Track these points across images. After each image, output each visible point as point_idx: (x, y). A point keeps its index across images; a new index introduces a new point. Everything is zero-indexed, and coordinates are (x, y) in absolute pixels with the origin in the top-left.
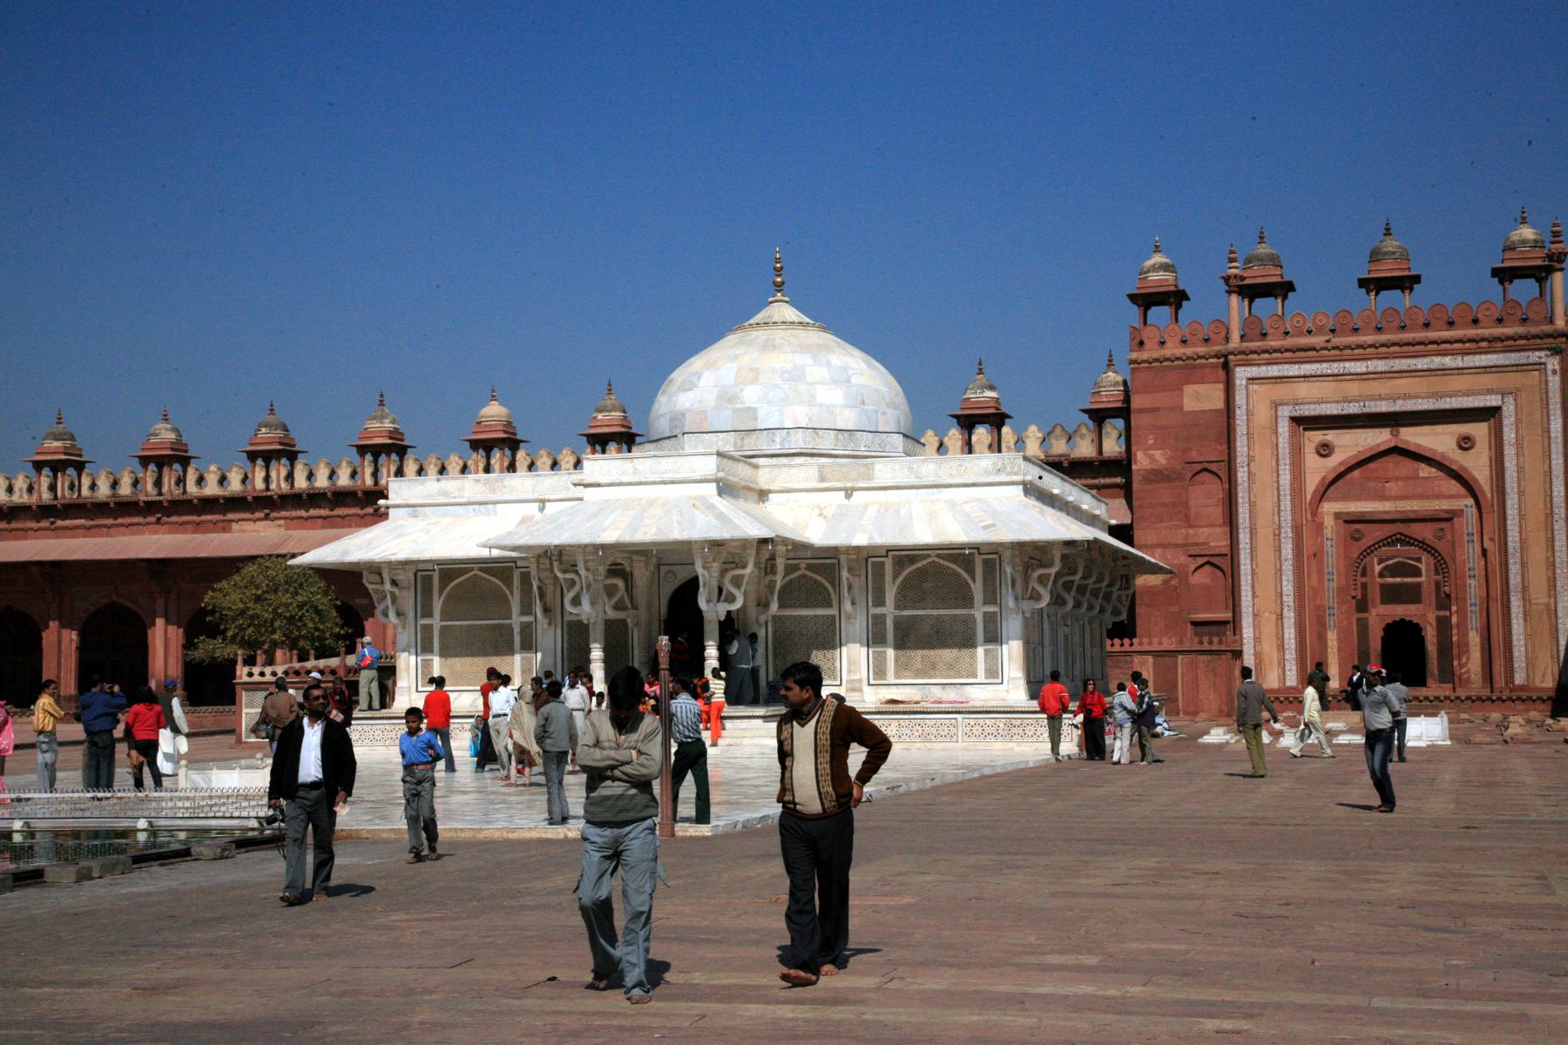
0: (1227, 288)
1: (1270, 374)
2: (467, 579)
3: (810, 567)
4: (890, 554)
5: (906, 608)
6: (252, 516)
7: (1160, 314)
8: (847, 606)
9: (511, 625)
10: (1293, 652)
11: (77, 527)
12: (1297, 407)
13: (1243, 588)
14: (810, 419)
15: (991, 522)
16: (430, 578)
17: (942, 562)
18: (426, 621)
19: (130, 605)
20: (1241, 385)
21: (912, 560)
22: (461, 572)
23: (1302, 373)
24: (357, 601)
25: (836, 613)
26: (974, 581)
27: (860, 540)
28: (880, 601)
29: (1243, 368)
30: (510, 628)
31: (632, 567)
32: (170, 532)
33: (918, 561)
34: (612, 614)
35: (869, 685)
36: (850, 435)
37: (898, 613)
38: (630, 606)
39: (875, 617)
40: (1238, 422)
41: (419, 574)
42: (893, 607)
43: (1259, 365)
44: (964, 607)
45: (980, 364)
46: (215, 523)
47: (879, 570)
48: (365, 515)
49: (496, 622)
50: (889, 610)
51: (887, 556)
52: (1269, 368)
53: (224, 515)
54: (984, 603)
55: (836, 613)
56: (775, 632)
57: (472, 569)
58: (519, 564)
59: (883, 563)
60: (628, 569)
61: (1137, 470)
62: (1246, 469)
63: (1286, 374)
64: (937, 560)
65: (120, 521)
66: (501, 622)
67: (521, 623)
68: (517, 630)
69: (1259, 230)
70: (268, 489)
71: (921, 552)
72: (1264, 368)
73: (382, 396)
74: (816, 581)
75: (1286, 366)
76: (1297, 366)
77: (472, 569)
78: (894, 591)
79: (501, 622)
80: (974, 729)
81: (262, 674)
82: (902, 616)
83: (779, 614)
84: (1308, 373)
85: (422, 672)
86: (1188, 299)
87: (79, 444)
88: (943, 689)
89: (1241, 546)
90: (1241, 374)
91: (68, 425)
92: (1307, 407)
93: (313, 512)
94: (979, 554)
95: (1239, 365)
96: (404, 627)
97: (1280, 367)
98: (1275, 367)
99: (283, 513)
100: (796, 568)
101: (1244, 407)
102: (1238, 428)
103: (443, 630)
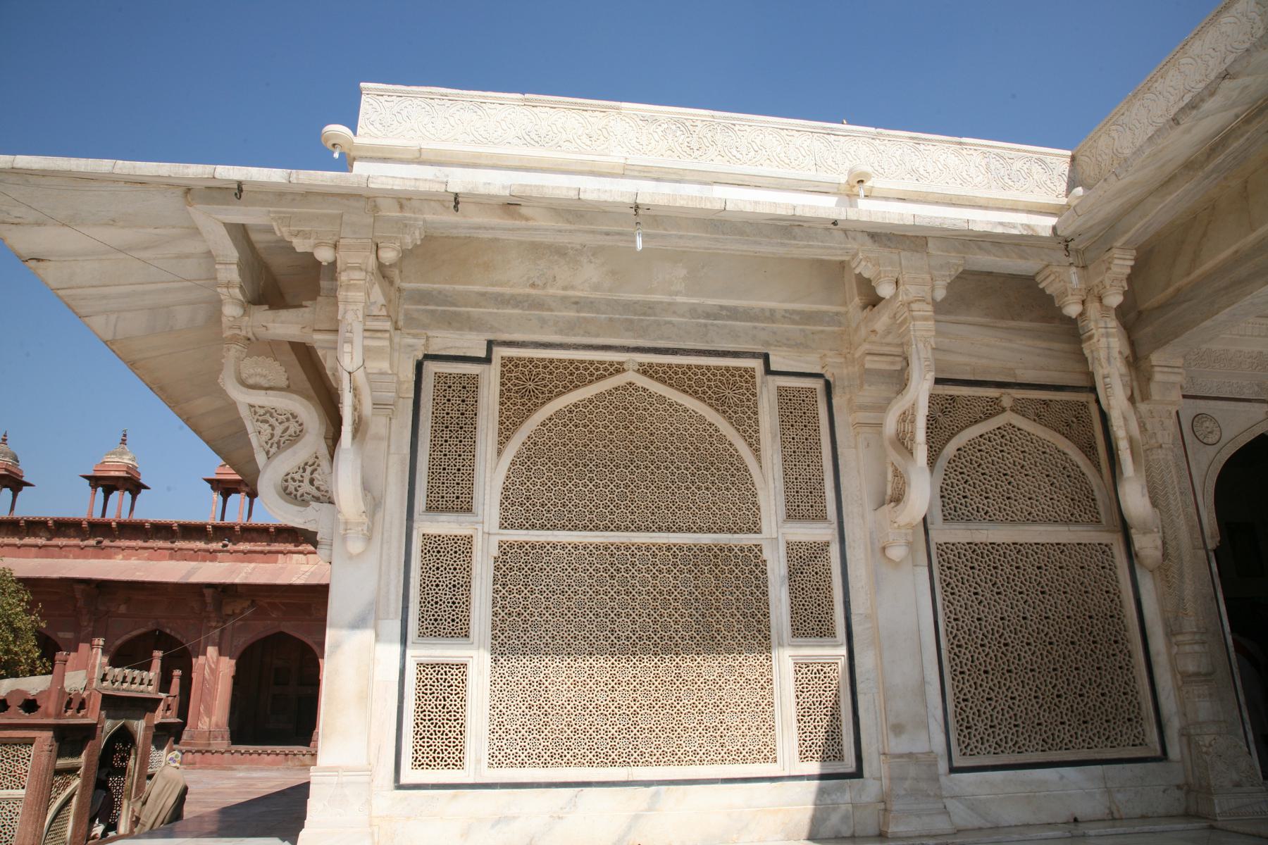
2: (600, 396)
16: (470, 386)
18: (446, 526)
22: (579, 375)
24: (61, 635)
30: (753, 562)
41: (431, 368)
48: (86, 546)
49: (706, 539)
57: (619, 369)
68: (777, 569)
73: (125, 435)
77: (619, 369)
85: (420, 710)
93: (27, 540)
96: (369, 539)
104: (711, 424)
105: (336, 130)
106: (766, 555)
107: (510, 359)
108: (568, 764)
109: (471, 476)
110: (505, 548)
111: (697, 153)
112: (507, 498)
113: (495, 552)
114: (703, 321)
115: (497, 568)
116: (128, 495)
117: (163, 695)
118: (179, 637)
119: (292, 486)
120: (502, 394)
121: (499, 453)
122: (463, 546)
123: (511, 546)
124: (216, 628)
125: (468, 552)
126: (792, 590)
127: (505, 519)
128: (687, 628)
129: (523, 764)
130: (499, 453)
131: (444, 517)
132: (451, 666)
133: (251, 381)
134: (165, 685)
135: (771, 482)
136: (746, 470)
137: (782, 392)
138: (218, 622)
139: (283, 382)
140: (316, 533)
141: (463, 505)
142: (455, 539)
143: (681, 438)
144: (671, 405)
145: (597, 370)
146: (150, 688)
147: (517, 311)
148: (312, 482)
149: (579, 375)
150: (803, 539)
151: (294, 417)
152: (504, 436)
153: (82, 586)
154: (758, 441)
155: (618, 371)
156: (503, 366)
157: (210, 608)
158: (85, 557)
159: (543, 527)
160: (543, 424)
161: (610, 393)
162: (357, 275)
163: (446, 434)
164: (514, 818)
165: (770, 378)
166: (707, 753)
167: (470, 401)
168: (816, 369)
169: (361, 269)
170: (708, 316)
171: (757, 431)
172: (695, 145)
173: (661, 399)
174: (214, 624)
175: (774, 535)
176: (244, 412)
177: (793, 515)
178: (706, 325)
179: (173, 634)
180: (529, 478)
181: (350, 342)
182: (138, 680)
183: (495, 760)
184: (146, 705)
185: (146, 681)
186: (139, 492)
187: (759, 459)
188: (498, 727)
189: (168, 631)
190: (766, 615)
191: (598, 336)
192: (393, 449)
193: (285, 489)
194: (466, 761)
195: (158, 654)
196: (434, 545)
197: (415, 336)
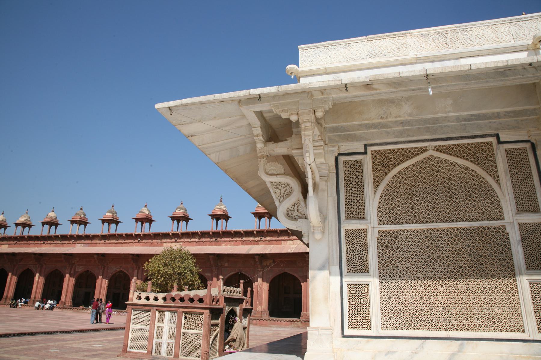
2: (417, 163)
6: (171, 241)
11: (112, 243)
16: (359, 165)
18: (355, 225)
19: (126, 272)
24: (206, 274)
32: (142, 246)
41: (342, 159)
46: (158, 243)
48: (212, 241)
49: (476, 224)
53: (161, 240)
57: (425, 150)
65: (126, 241)
66: (485, 223)
68: (515, 237)
73: (221, 198)
77: (425, 150)
79: (485, 223)
81: (148, 298)
85: (350, 304)
87: (118, 215)
91: (115, 209)
93: (193, 240)
96: (323, 232)
99: (182, 240)
103: (383, 237)
104: (472, 171)
105: (291, 67)
106: (508, 230)
107: (375, 151)
108: (418, 329)
109: (363, 203)
110: (382, 234)
111: (450, 46)
112: (380, 212)
113: (377, 235)
114: (463, 123)
115: (379, 242)
116: (224, 221)
117: (245, 297)
118: (247, 275)
119: (290, 213)
120: (373, 167)
121: (375, 192)
122: (363, 234)
123: (384, 232)
124: (260, 271)
125: (365, 236)
126: (524, 247)
127: (380, 221)
128: (470, 266)
129: (397, 328)
130: (375, 192)
131: (354, 222)
132: (362, 285)
133: (270, 172)
134: (245, 294)
135: (507, 195)
136: (493, 190)
137: (507, 151)
138: (261, 269)
139: (283, 172)
140: (301, 232)
141: (361, 216)
142: (359, 231)
143: (458, 178)
144: (452, 163)
145: (415, 151)
146: (240, 295)
147: (375, 130)
148: (298, 211)
150: (528, 221)
151: (288, 185)
152: (376, 184)
153: (212, 256)
154: (498, 176)
155: (424, 151)
156: (372, 154)
157: (258, 263)
158: (212, 245)
159: (397, 223)
160: (393, 178)
161: (422, 161)
162: (308, 124)
163: (351, 186)
164: (395, 352)
165: (501, 145)
166: (486, 326)
167: (360, 171)
168: (526, 138)
169: (309, 122)
170: (465, 120)
171: (497, 172)
172: (449, 42)
173: (447, 161)
174: (260, 270)
175: (512, 221)
176: (269, 185)
177: (520, 210)
178: (465, 125)
179: (245, 274)
180: (389, 202)
181: (308, 152)
182: (236, 292)
183: (384, 326)
184: (239, 301)
185: (238, 292)
186: (228, 220)
187: (499, 184)
188: (384, 311)
189: (243, 273)
190: (511, 259)
191: (413, 136)
192: (329, 195)
193: (288, 214)
194: (372, 326)
195: (242, 282)
196: (350, 234)
197: (334, 146)
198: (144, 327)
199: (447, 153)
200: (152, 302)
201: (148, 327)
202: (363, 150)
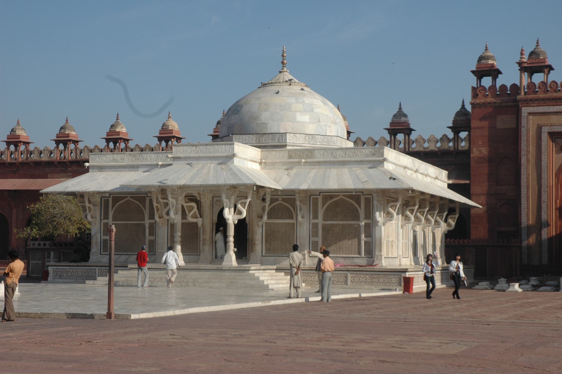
0: (519, 68)
1: (539, 111)
2: (125, 202)
3: (283, 200)
4: (321, 194)
5: (328, 220)
7: (487, 82)
8: (300, 218)
9: (144, 223)
10: (546, 247)
12: (552, 127)
13: (523, 216)
14: (292, 129)
15: (367, 179)
16: (108, 200)
17: (345, 198)
18: (105, 221)
20: (524, 116)
21: (331, 197)
22: (122, 198)
23: (555, 110)
25: (295, 222)
26: (360, 208)
27: (304, 187)
28: (316, 217)
29: (526, 108)
30: (144, 225)
31: (200, 197)
33: (334, 198)
34: (190, 219)
35: (310, 257)
36: (312, 137)
37: (324, 222)
38: (199, 216)
39: (313, 224)
40: (522, 134)
41: (103, 199)
42: (322, 219)
43: (534, 106)
44: (355, 220)
45: (400, 104)
47: (316, 201)
49: (137, 222)
50: (320, 221)
51: (320, 195)
52: (539, 108)
54: (365, 218)
55: (295, 222)
56: (266, 230)
57: (127, 197)
58: (148, 196)
59: (318, 198)
60: (199, 199)
61: (473, 157)
62: (525, 157)
63: (547, 111)
64: (343, 197)
67: (149, 223)
68: (147, 226)
69: (537, 40)
70: (76, 157)
71: (336, 194)
72: (536, 108)
73: (118, 115)
74: (286, 206)
75: (547, 107)
76: (552, 107)
77: (127, 197)
78: (322, 212)
80: (355, 279)
82: (326, 224)
83: (269, 222)
84: (557, 111)
86: (501, 73)
88: (344, 259)
89: (522, 195)
90: (525, 110)
92: (557, 127)
94: (363, 195)
95: (524, 106)
97: (544, 107)
98: (541, 107)
100: (277, 200)
101: (526, 127)
102: (522, 137)
106: (145, 224)
121: (112, 210)
149: (122, 198)
173: (133, 202)
198: (39, 262)
199: (133, 199)
200: (42, 246)
201: (41, 262)
202: (109, 196)
